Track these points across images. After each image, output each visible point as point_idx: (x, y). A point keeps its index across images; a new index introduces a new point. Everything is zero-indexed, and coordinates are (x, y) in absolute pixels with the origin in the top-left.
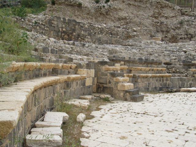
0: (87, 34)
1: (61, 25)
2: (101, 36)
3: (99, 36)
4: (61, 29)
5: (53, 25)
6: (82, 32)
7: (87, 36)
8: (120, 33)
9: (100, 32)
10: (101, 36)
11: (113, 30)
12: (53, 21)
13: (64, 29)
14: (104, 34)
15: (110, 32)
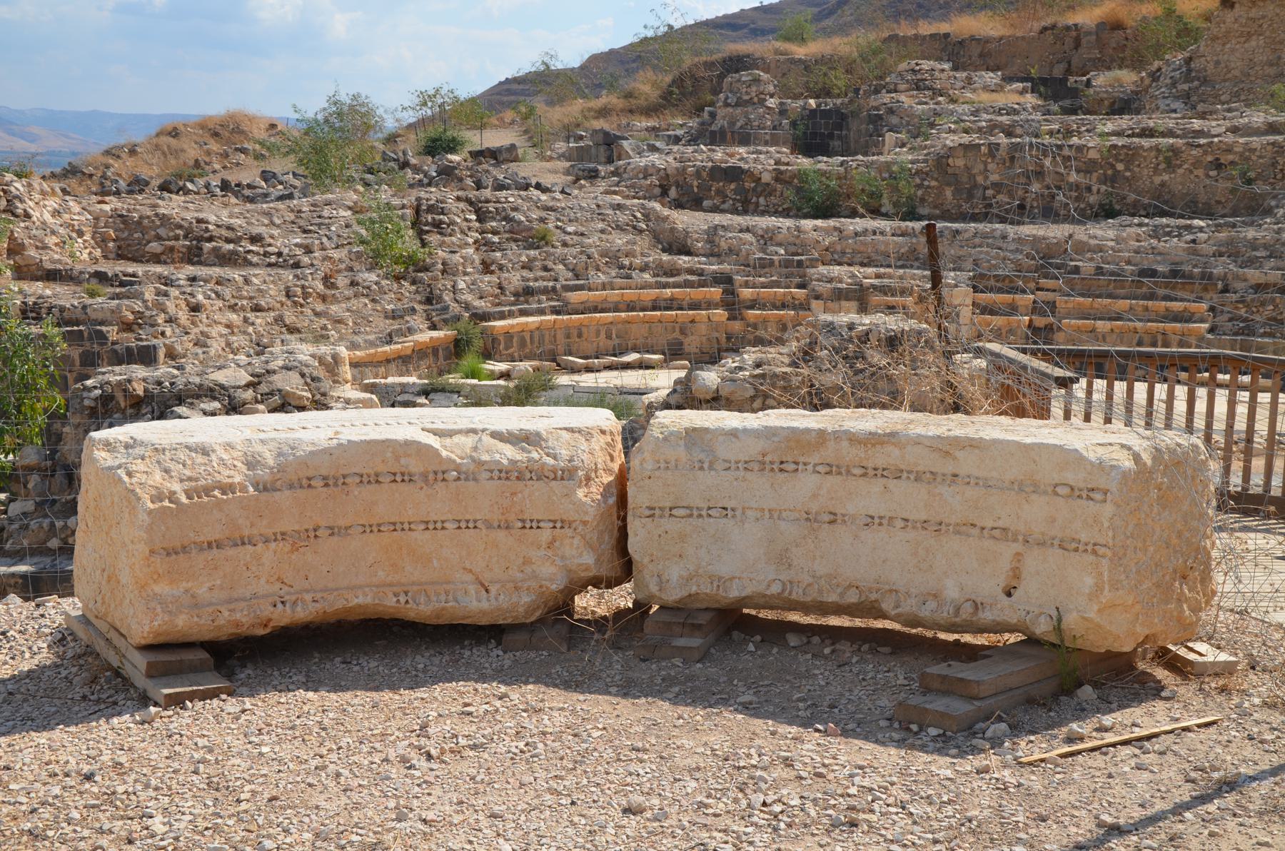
0: (1094, 179)
1: (981, 167)
2: (1166, 177)
3: (1157, 180)
4: (980, 179)
5: (950, 171)
6: (1073, 177)
7: (1095, 189)
8: (1260, 157)
9: (1162, 166)
10: (1166, 177)
11: (1229, 150)
12: (950, 161)
13: (995, 178)
14: (1180, 171)
15: (1210, 158)
